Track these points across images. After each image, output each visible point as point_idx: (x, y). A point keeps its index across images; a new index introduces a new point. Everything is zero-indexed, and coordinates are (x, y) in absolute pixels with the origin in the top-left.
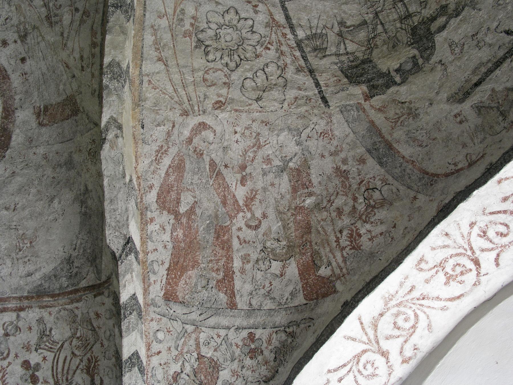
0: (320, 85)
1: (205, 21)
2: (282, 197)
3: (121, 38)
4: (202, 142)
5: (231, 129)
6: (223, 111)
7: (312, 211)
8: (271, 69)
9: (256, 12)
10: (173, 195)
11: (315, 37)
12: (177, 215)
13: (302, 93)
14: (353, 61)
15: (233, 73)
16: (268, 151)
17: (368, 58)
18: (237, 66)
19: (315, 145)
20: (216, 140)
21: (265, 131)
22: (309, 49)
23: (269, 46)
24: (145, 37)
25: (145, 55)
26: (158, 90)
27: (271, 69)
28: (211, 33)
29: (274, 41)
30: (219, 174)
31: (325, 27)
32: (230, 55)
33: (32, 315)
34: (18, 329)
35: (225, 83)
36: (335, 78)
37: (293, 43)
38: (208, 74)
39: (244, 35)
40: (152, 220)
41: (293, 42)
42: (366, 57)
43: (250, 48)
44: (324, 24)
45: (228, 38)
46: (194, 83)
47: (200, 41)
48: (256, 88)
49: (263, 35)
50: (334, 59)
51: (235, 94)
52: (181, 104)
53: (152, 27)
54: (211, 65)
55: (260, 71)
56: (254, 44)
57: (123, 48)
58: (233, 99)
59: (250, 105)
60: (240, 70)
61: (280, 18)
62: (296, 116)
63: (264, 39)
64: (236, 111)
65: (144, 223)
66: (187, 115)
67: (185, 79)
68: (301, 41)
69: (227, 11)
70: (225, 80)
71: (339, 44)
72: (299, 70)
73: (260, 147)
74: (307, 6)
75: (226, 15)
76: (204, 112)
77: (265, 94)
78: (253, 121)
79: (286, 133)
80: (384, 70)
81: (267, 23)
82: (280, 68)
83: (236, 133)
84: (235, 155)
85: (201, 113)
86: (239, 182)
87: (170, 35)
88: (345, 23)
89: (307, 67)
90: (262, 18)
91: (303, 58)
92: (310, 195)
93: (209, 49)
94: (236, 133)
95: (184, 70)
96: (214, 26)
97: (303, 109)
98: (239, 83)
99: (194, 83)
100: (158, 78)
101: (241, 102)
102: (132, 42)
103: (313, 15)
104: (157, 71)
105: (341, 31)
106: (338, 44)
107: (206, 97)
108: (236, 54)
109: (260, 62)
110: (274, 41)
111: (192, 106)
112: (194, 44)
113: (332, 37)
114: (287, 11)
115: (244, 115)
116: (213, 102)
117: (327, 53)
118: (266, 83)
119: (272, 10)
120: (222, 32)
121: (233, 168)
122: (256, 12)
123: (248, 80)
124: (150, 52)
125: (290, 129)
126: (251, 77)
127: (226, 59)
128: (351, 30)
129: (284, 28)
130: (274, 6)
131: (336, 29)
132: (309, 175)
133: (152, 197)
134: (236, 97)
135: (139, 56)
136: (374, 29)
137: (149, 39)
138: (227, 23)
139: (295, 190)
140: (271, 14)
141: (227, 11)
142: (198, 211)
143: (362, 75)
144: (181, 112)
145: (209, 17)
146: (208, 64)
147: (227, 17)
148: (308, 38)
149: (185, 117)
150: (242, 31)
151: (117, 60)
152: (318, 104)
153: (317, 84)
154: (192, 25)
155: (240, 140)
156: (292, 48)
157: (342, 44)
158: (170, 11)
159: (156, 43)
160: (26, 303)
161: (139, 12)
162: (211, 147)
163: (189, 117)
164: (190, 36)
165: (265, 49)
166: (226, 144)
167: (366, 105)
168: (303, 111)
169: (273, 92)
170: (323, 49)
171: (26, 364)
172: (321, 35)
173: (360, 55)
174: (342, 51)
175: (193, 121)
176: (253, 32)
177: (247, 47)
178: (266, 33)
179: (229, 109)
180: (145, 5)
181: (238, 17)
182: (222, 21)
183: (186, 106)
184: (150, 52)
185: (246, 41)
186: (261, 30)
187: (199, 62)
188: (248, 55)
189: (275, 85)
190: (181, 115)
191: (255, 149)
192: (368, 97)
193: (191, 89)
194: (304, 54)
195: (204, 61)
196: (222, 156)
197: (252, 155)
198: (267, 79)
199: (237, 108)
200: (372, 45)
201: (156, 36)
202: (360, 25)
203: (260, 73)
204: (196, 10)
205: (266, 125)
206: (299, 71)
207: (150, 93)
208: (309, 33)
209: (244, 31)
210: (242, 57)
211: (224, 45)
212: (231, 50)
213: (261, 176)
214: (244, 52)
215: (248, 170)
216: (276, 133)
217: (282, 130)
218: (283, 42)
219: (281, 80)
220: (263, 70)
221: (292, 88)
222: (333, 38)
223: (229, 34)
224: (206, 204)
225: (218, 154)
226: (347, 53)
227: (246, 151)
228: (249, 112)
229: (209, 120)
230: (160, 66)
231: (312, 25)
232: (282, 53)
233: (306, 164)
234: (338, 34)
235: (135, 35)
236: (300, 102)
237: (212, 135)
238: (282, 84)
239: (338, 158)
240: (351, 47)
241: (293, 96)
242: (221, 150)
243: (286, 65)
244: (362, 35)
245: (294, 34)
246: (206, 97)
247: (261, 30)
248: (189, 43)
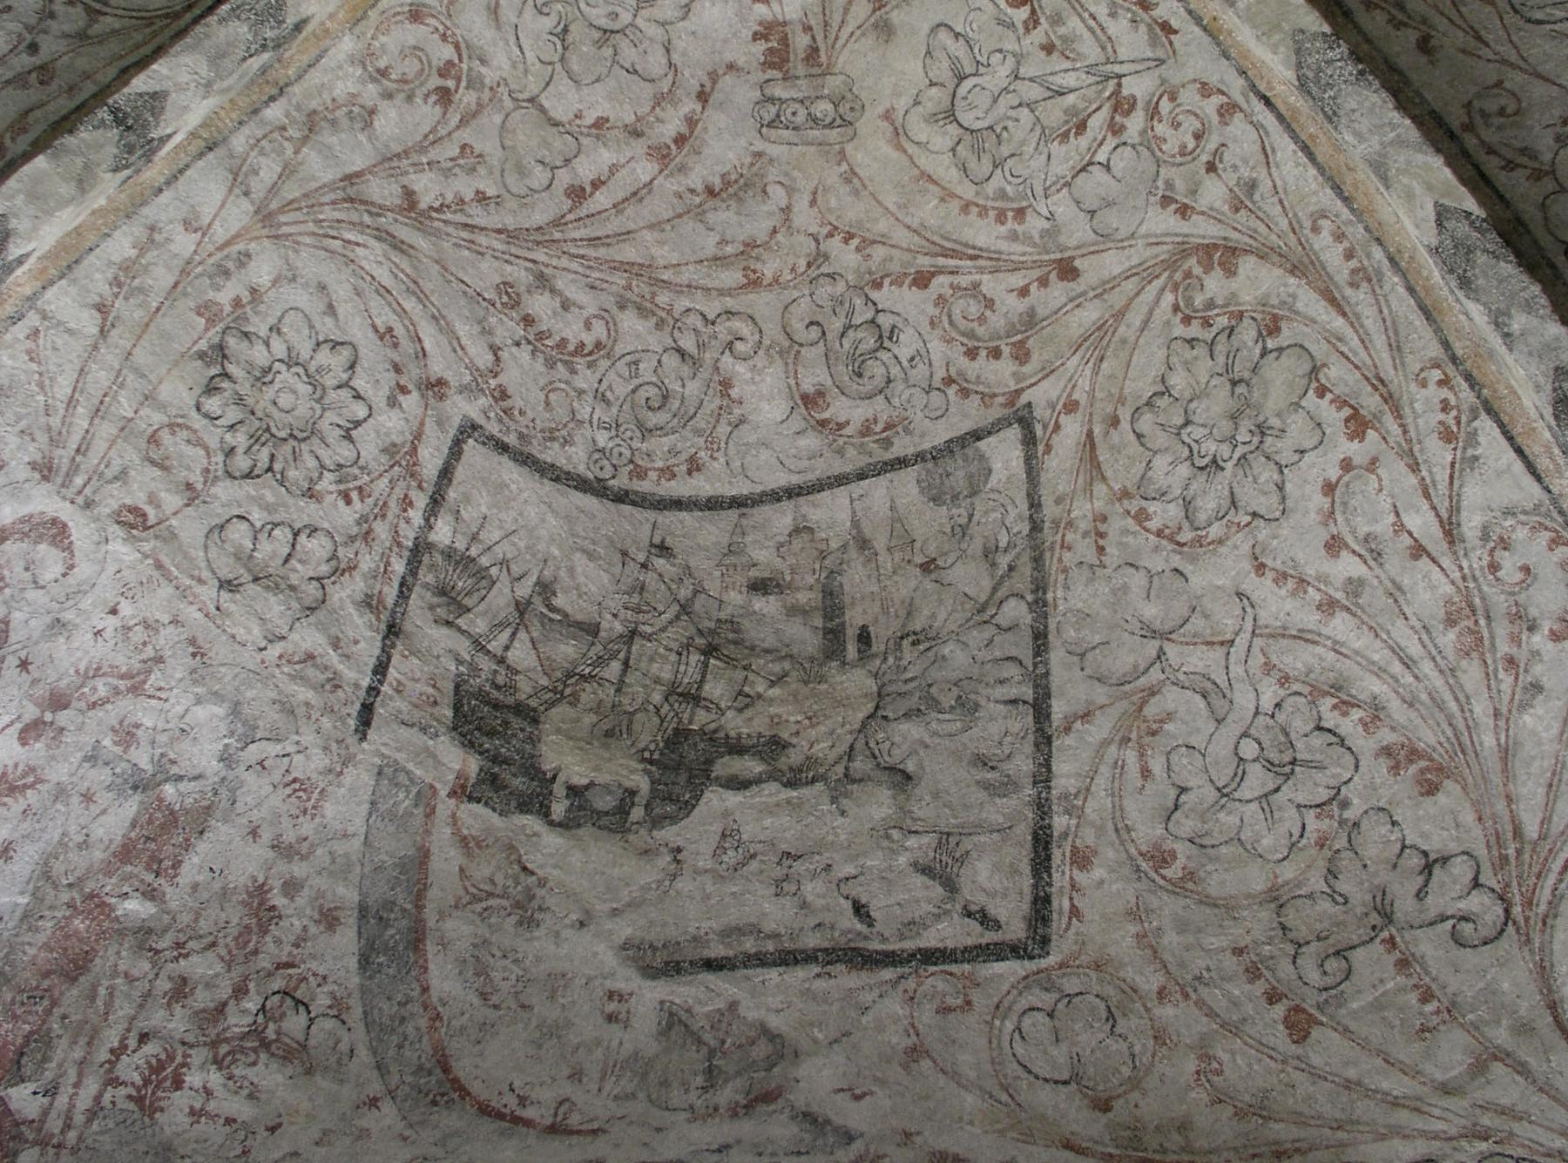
0: (384, 676)
1: (272, 321)
2: (84, 845)
3: (66, 190)
4: (22, 564)
5: (111, 597)
6: (130, 539)
7: (122, 933)
8: (316, 547)
9: (392, 402)
11: (466, 567)
13: (333, 658)
14: (498, 687)
15: (228, 482)
16: (146, 714)
17: (535, 710)
19: (259, 795)
20: (55, 590)
21: (179, 666)
22: (430, 579)
23: (354, 495)
24: (117, 234)
25: (79, 271)
26: (34, 366)
27: (316, 547)
28: (259, 355)
29: (376, 495)
31: (504, 563)
32: (255, 438)
35: (189, 486)
36: (430, 690)
37: (408, 536)
38: (173, 433)
39: (324, 425)
41: (412, 535)
42: (533, 703)
43: (312, 463)
44: (509, 556)
45: (285, 400)
46: (126, 426)
48: (244, 558)
49: (362, 462)
50: (464, 647)
51: (190, 528)
52: (55, 441)
53: (152, 229)
54: (198, 422)
55: (287, 530)
56: (327, 462)
57: (50, 213)
58: (174, 536)
59: (200, 581)
60: (249, 487)
61: (430, 460)
62: (273, 695)
63: (356, 471)
64: (159, 566)
66: (45, 478)
67: (114, 398)
68: (430, 546)
69: (335, 345)
70: (197, 478)
71: (502, 625)
72: (369, 603)
73: (135, 690)
74: (507, 486)
75: (325, 348)
76: (88, 505)
77: (253, 589)
78: (174, 621)
79: (220, 711)
80: (548, 766)
81: (395, 445)
82: (334, 563)
83: (114, 612)
84: (65, 658)
85: (80, 500)
86: (18, 726)
87: (171, 280)
88: (554, 594)
89: (394, 612)
90: (392, 424)
91: (402, 585)
92: (151, 894)
93: (225, 384)
94: (114, 612)
95: (131, 377)
96: (279, 348)
97: (304, 694)
98: (221, 513)
99: (126, 426)
100: (59, 342)
101: (186, 556)
102: (81, 219)
103: (503, 516)
104: (72, 325)
105: (529, 603)
106: (501, 624)
107: (122, 476)
108: (270, 447)
109: (305, 512)
110: (376, 495)
111: (74, 468)
112: (203, 345)
113: (501, 598)
114: (457, 460)
115: (167, 590)
116: (128, 501)
117: (460, 622)
118: (275, 566)
119: (430, 427)
120: (285, 376)
121: (35, 682)
122: (392, 402)
123: (244, 526)
124: (96, 275)
125: (235, 711)
126: (258, 524)
127: (240, 439)
128: (551, 620)
129: (420, 487)
130: (440, 423)
131: (524, 590)
132: (187, 846)
134: (184, 536)
135: (67, 260)
136: (600, 661)
137: (121, 246)
138: (312, 369)
139: (126, 853)
140: (418, 436)
141: (335, 345)
143: (491, 734)
144: (38, 457)
145: (286, 320)
146: (194, 413)
147: (324, 357)
148: (449, 553)
149: (37, 476)
150: (328, 414)
151: (13, 223)
152: (345, 711)
153: (381, 669)
154: (237, 303)
155: (108, 634)
156: (399, 545)
157: (509, 631)
158: (220, 233)
159: (128, 267)
161: (155, 172)
162: (32, 594)
163: (46, 486)
164: (211, 322)
165: (340, 492)
166: (69, 616)
167: (445, 806)
168: (301, 697)
169: (273, 599)
170: (460, 605)
172: (481, 574)
173: (525, 687)
174: (495, 646)
175: (45, 502)
176: (348, 437)
177: (306, 456)
178: (373, 465)
179: (147, 547)
180: (181, 172)
181: (345, 376)
182: (305, 354)
183: (63, 456)
184: (96, 275)
185: (315, 440)
186: (369, 445)
187: (178, 391)
188: (292, 473)
189: (292, 588)
190: (33, 466)
191: (122, 684)
192: (462, 792)
193: (106, 430)
194: (410, 580)
195: (189, 399)
196: (36, 635)
197: (102, 691)
198: (286, 561)
199: (166, 561)
200: (568, 691)
201: (142, 251)
202: (579, 625)
204: (275, 282)
205: (194, 655)
206: (369, 605)
207: (11, 357)
208: (460, 545)
209: (330, 416)
210: (277, 467)
211: (262, 403)
212: (268, 429)
213: (79, 755)
214: (290, 458)
215: (63, 718)
216: (199, 690)
217: (217, 697)
218: (390, 515)
219: (312, 589)
220: (296, 534)
221: (322, 627)
222: (502, 602)
223: (294, 392)
225: (33, 623)
226: (501, 661)
227: (98, 672)
228: (183, 593)
229: (81, 531)
230: (88, 323)
231: (482, 536)
232: (367, 536)
233: (201, 819)
234: (517, 604)
235: (101, 209)
236: (311, 672)
237: (59, 569)
238: (308, 602)
239: (282, 868)
240: (521, 654)
241: (307, 645)
242: (48, 619)
243: (352, 568)
244: (567, 650)
245: (427, 520)
246: (122, 476)
247: (369, 445)
248: (194, 332)
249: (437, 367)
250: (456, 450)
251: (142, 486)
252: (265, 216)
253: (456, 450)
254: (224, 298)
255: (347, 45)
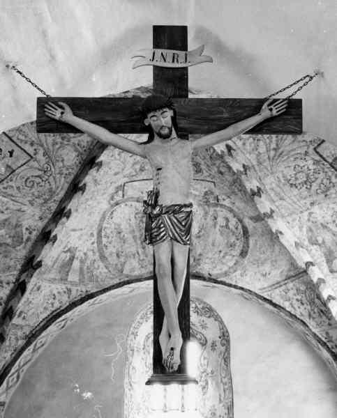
8: (325, 181)
10: (313, 239)
12: (320, 245)
18: (311, 186)
27: (325, 181)
30: (326, 227)
32: (306, 184)
33: (290, 285)
34: (289, 290)
37: (329, 166)
40: (311, 250)
47: (291, 184)
61: (318, 158)
65: (309, 251)
69: (295, 168)
90: (310, 162)
99: (298, 200)
108: (308, 182)
109: (319, 181)
122: (306, 161)
127: (305, 186)
133: (306, 243)
142: (326, 241)
160: (286, 282)
161: (262, 188)
171: (297, 300)
176: (310, 170)
186: (311, 167)
187: (295, 191)
195: (297, 190)
203: (322, 185)
219: (331, 184)
224: (327, 237)
229: (312, 211)
232: (326, 172)
247: (311, 167)
248: (287, 188)
249: (303, 152)
250: (317, 153)
251: (308, 201)
252: (272, 173)
253: (317, 153)
254: (283, 181)
255: (248, 155)
